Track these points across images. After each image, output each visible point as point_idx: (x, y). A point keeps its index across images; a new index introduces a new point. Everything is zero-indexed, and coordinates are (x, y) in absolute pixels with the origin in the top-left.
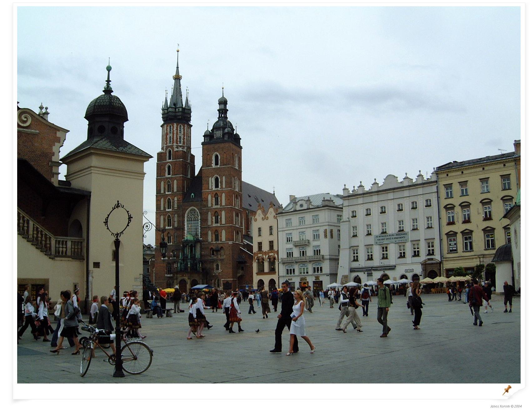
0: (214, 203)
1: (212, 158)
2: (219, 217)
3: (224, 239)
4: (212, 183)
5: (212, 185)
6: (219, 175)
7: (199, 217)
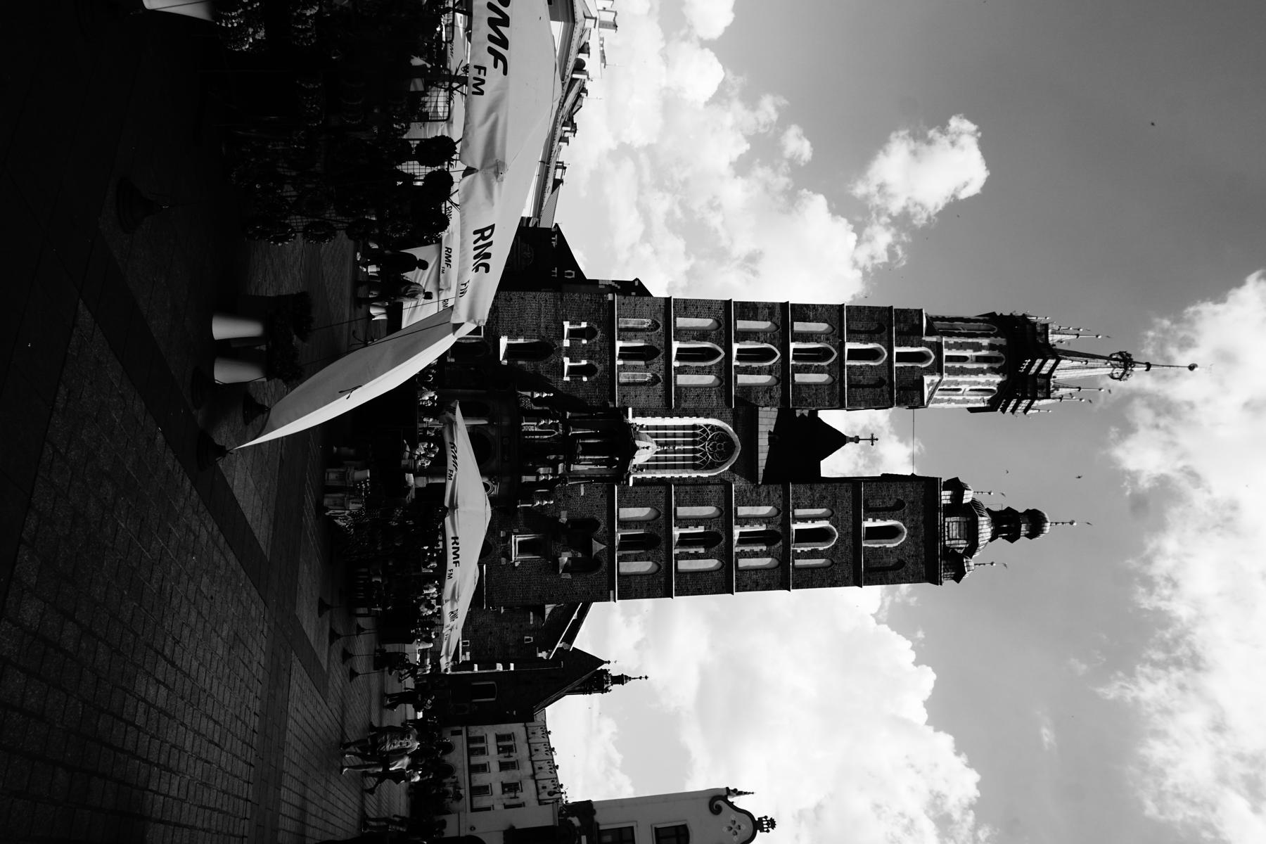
0: (747, 529)
2: (702, 550)
4: (813, 522)
5: (804, 519)
6: (835, 547)
7: (705, 475)
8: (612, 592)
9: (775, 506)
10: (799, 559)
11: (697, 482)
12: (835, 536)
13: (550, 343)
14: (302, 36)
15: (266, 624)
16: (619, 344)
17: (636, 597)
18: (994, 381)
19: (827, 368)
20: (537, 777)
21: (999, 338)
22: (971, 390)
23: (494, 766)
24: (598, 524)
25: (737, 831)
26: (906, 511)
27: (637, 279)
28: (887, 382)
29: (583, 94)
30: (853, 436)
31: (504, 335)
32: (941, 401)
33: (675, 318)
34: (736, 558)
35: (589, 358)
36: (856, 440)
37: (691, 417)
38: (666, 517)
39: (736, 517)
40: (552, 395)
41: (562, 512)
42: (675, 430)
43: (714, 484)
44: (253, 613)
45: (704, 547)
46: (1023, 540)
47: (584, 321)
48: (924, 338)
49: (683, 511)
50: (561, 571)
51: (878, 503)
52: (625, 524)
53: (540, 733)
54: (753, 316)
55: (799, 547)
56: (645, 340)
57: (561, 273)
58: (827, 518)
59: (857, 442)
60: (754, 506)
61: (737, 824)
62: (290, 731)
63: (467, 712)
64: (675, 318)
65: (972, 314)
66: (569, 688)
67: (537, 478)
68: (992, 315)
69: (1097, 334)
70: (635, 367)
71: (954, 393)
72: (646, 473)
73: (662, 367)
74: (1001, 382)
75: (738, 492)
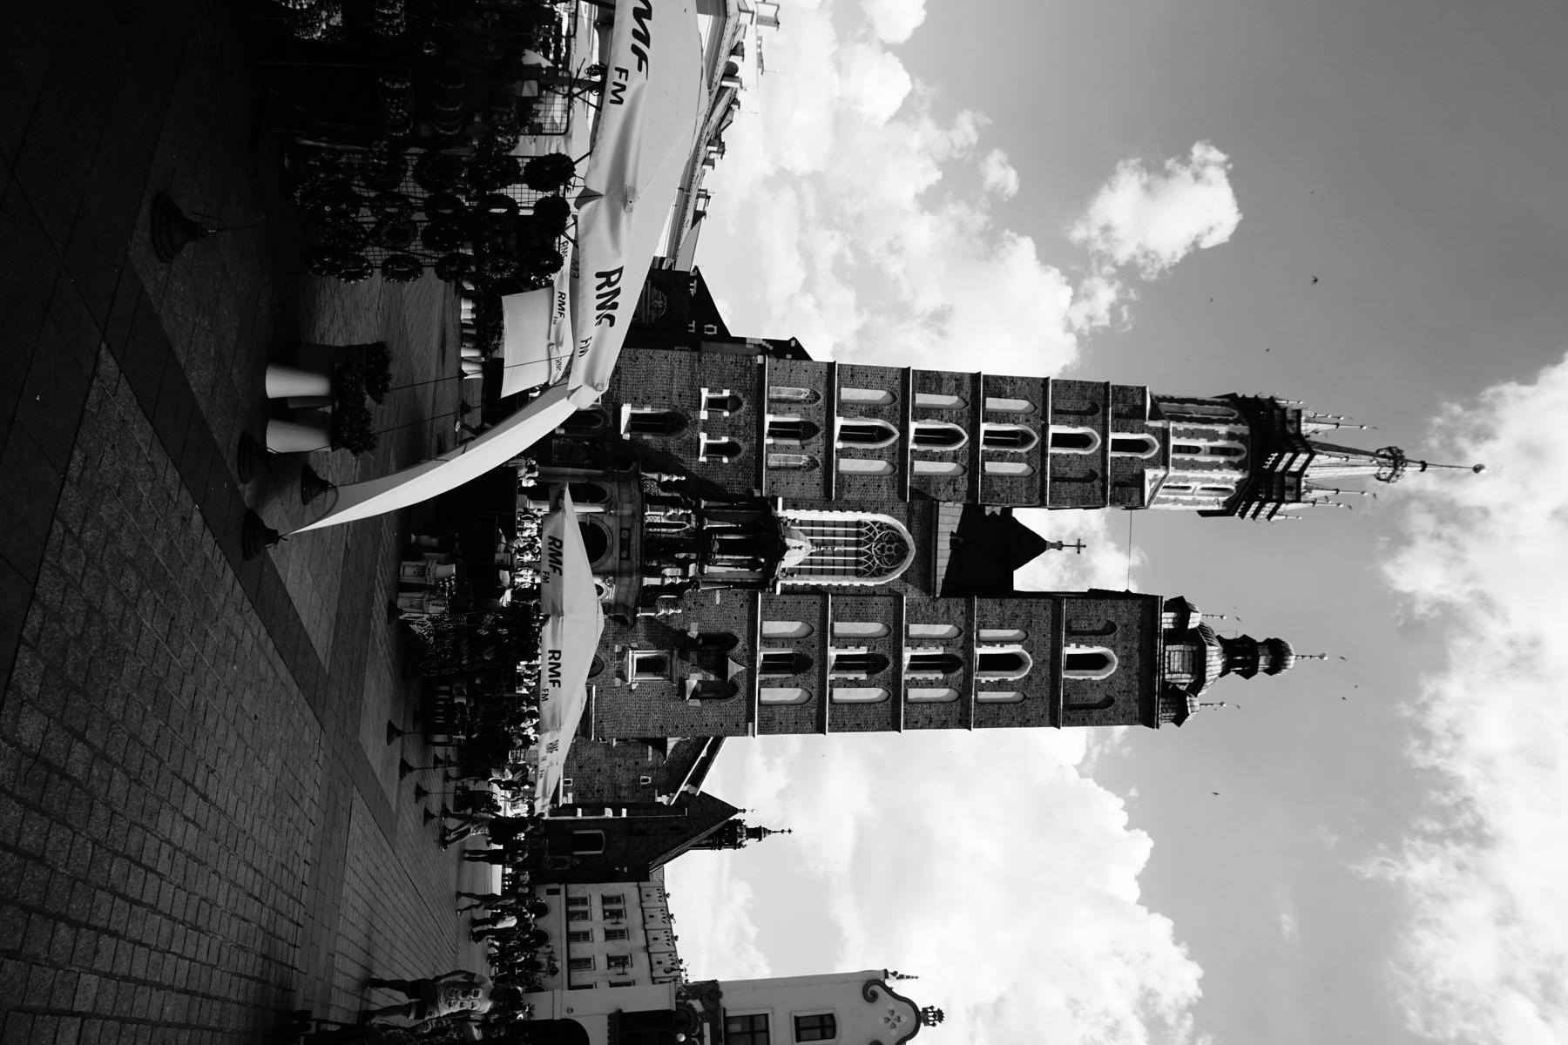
0: (921, 652)
1: (1099, 644)
2: (863, 677)
3: (769, 695)
4: (1002, 646)
6: (1028, 678)
7: (870, 583)
8: (750, 724)
9: (955, 625)
10: (983, 690)
11: (860, 592)
12: (1029, 663)
13: (684, 414)
14: (387, 24)
15: (321, 751)
16: (769, 418)
17: (780, 732)
18: (1232, 478)
19: (1026, 456)
20: (651, 950)
21: (1240, 426)
22: (1203, 489)
23: (599, 935)
24: (736, 641)
25: (897, 1023)
26: (1118, 636)
27: (793, 339)
28: (1100, 476)
29: (734, 107)
30: (1056, 542)
31: (626, 403)
32: (1166, 501)
33: (839, 388)
34: (905, 687)
35: (732, 434)
36: (1059, 546)
37: (855, 511)
38: (822, 634)
39: (907, 636)
40: (684, 478)
41: (692, 624)
42: (835, 526)
43: (880, 595)
44: (306, 738)
45: (867, 673)
46: (1261, 676)
47: (726, 388)
48: (1146, 423)
49: (842, 628)
50: (688, 697)
51: (1083, 625)
52: (769, 641)
53: (656, 895)
54: (935, 389)
55: (984, 676)
56: (802, 415)
57: (700, 328)
58: (1019, 642)
59: (1059, 549)
60: (929, 624)
61: (896, 1015)
62: (349, 884)
63: (566, 867)
64: (839, 388)
65: (1207, 396)
66: (694, 841)
67: (663, 582)
68: (1233, 397)
69: (1361, 424)
70: (788, 447)
71: (1182, 491)
72: (797, 579)
73: (822, 449)
74: (1241, 480)
75: (913, 607)
